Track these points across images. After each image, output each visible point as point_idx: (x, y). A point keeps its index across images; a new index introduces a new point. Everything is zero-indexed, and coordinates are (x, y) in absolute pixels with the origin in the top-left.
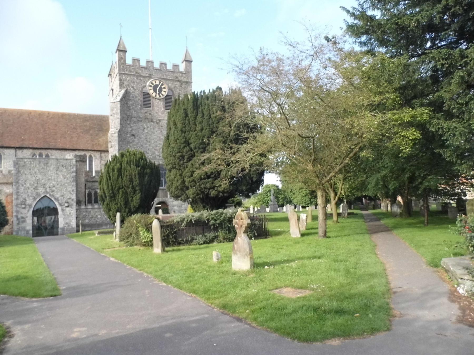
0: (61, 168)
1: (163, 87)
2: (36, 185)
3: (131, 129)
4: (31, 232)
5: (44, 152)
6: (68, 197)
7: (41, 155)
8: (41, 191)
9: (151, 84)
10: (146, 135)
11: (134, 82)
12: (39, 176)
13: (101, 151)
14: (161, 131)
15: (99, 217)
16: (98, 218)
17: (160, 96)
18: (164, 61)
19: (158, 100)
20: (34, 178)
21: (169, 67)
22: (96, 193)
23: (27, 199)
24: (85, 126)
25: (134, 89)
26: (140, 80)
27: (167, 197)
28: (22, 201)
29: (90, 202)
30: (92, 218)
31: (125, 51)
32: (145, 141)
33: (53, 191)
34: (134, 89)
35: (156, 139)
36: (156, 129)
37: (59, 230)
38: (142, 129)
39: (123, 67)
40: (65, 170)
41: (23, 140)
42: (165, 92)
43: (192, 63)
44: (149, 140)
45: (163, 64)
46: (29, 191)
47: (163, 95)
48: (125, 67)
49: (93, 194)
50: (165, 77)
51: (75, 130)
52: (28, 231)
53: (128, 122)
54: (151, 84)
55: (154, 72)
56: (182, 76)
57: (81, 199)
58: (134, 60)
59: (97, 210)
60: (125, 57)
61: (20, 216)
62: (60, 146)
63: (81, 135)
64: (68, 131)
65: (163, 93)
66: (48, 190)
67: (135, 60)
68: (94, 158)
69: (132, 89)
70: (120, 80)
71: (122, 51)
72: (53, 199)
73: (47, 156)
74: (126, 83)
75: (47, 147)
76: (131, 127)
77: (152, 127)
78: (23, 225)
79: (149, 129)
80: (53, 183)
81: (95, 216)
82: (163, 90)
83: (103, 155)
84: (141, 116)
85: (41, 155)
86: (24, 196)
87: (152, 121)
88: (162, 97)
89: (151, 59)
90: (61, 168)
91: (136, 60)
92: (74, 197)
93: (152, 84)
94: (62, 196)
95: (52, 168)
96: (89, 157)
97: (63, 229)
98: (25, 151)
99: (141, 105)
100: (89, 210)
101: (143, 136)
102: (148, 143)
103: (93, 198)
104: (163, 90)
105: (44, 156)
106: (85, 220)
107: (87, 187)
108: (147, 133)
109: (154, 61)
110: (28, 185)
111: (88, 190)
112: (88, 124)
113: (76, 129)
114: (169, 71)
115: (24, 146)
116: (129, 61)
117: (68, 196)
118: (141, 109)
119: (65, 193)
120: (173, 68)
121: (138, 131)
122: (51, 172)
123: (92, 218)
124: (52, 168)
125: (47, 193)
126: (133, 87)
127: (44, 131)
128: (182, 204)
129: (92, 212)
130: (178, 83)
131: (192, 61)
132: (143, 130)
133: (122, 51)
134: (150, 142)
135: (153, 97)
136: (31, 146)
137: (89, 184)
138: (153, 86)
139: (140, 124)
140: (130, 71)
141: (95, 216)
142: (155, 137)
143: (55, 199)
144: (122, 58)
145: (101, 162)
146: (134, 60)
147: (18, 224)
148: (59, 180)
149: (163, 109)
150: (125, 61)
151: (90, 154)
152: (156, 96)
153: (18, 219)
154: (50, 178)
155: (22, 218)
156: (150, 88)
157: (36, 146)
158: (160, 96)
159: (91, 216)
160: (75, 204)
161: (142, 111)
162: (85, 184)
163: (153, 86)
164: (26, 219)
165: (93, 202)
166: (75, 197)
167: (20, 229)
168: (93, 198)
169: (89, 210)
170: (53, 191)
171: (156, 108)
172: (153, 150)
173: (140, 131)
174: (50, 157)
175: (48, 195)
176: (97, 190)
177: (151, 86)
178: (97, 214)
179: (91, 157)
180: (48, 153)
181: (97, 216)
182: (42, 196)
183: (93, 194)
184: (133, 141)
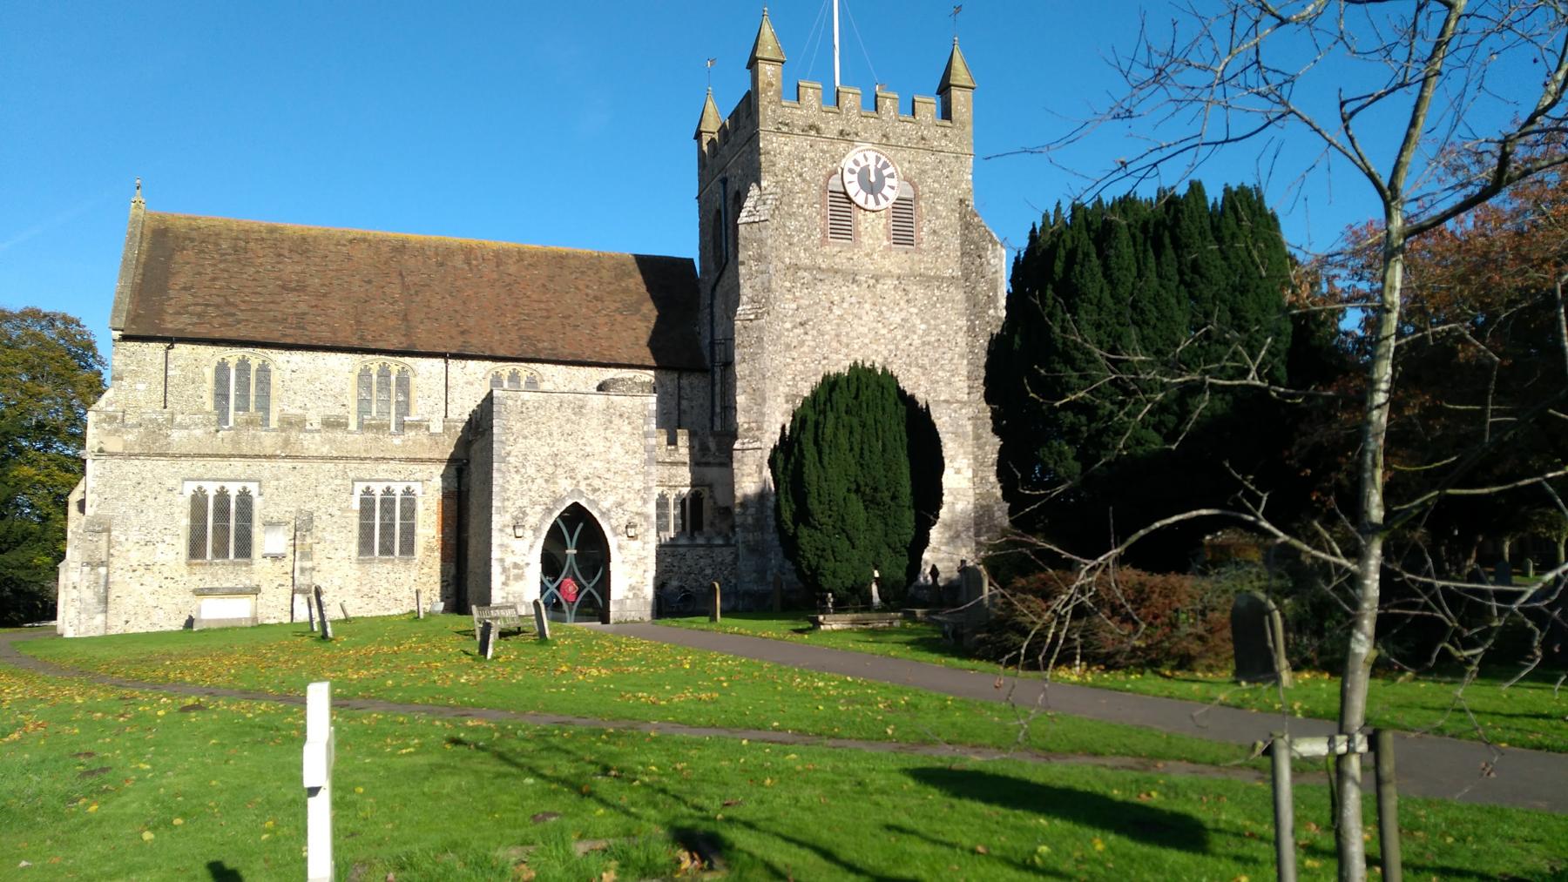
0: (616, 420)
2: (550, 470)
3: (794, 306)
5: (524, 369)
8: (564, 485)
12: (561, 446)
17: (878, 203)
20: (546, 448)
23: (528, 510)
24: (626, 291)
25: (804, 180)
26: (822, 151)
28: (515, 518)
32: (834, 344)
33: (595, 490)
34: (804, 180)
36: (867, 306)
40: (628, 429)
41: (463, 333)
44: (844, 340)
46: (535, 487)
51: (600, 305)
53: (788, 284)
59: (701, 551)
61: (508, 563)
62: (566, 352)
63: (620, 318)
65: (886, 191)
66: (583, 487)
69: (798, 180)
72: (596, 514)
73: (532, 385)
76: (795, 299)
77: (854, 300)
78: (515, 587)
79: (845, 305)
80: (595, 464)
83: (684, 382)
84: (823, 266)
85: (514, 377)
86: (518, 504)
87: (854, 281)
88: (883, 204)
90: (616, 420)
94: (619, 505)
95: (594, 423)
97: (621, 602)
98: (472, 365)
99: (823, 231)
100: (682, 550)
101: (828, 327)
102: (844, 350)
104: (888, 181)
108: (841, 317)
110: (531, 471)
117: (634, 505)
118: (823, 242)
119: (627, 496)
122: (592, 434)
124: (594, 423)
125: (581, 493)
127: (516, 305)
130: (929, 158)
132: (830, 310)
134: (848, 345)
139: (822, 288)
142: (861, 329)
145: (679, 404)
148: (612, 456)
149: (886, 243)
153: (504, 570)
154: (588, 449)
155: (516, 566)
158: (878, 203)
159: (685, 569)
161: (827, 249)
163: (857, 169)
169: (682, 550)
170: (595, 490)
171: (865, 240)
173: (821, 312)
175: (583, 503)
177: (852, 171)
178: (702, 562)
181: (702, 570)
182: (569, 503)
184: (802, 343)
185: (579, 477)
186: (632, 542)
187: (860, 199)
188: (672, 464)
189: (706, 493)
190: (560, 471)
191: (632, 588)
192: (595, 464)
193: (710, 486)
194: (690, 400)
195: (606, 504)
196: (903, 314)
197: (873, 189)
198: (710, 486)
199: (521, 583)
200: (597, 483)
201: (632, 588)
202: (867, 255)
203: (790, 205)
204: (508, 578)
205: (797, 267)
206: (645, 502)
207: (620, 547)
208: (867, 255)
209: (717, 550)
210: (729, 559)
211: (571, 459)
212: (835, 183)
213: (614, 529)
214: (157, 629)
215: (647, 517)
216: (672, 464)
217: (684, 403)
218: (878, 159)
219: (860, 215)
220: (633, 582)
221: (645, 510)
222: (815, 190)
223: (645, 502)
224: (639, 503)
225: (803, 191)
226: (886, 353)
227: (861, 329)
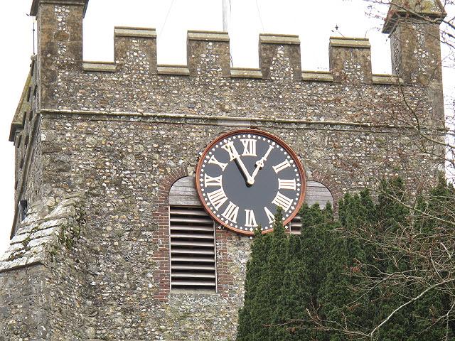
1: (277, 169)
9: (213, 160)
18: (280, 27)
21: (315, 59)
26: (155, 138)
39: (69, 81)
42: (288, 193)
54: (213, 160)
55: (229, 94)
58: (123, 38)
60: (77, 28)
65: (280, 200)
67: (129, 37)
69: (111, 191)
82: (283, 184)
93: (223, 156)
99: (159, 277)
109: (232, 38)
114: (314, 81)
116: (98, 47)
118: (158, 299)
120: (333, 62)
126: (117, 183)
138: (223, 166)
140: (104, 102)
146: (123, 38)
150: (77, 50)
156: (208, 180)
177: (214, 171)
187: (230, 215)
212: (181, 192)
218: (261, 150)
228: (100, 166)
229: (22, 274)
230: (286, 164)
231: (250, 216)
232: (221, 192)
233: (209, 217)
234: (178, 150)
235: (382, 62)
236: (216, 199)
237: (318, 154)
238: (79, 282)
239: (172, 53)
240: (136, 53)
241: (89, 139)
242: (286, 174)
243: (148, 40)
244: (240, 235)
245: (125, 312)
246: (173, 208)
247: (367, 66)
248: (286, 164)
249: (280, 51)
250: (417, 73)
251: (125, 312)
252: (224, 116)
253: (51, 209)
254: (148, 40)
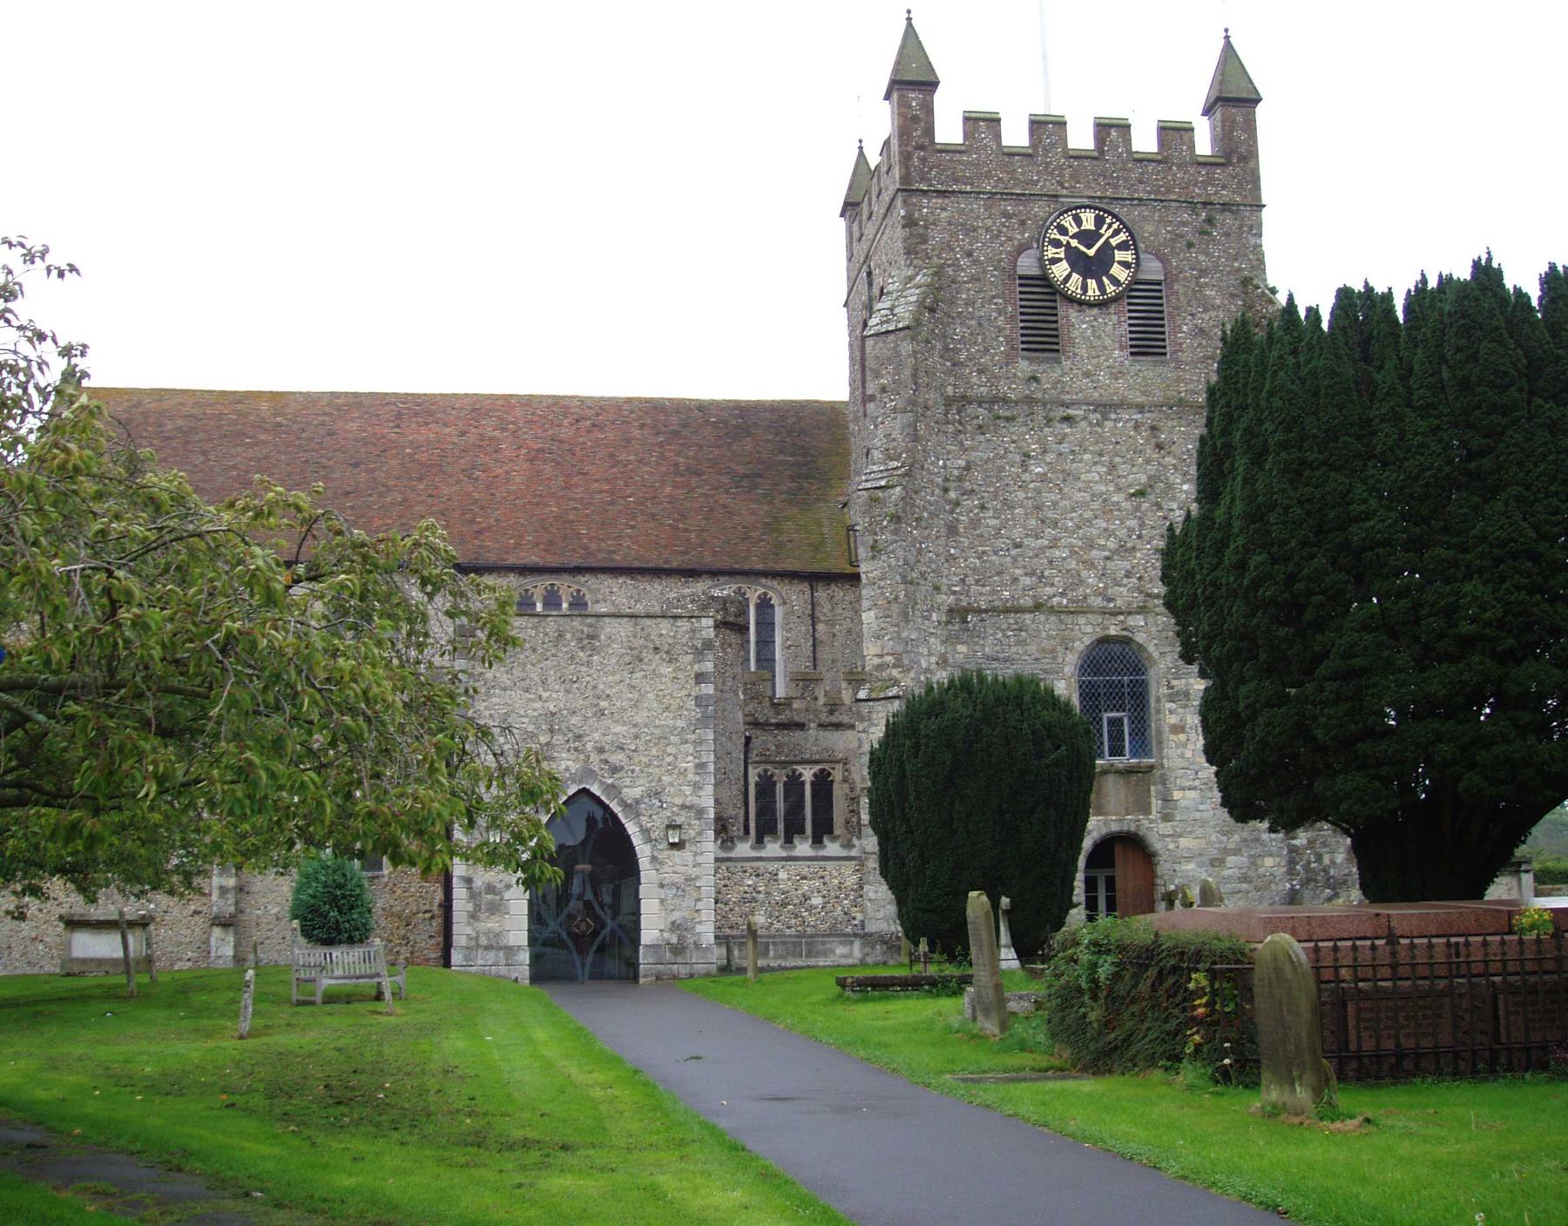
0: (647, 655)
2: (543, 739)
4: (525, 957)
5: (566, 587)
6: (678, 801)
7: (552, 600)
10: (1038, 491)
11: (975, 230)
13: (815, 579)
14: (1113, 467)
15: (817, 901)
16: (810, 909)
19: (1095, 311)
20: (538, 705)
21: (1145, 141)
22: (794, 783)
27: (1146, 810)
29: (765, 830)
30: (784, 905)
31: (934, 84)
32: (1033, 522)
33: (615, 770)
34: (976, 262)
35: (1086, 505)
36: (1087, 457)
37: (644, 958)
38: (1018, 459)
39: (923, 160)
40: (666, 670)
43: (1260, 110)
45: (1111, 131)
47: (1115, 281)
48: (932, 160)
49: (780, 788)
50: (1125, 193)
51: (694, 481)
52: (510, 950)
56: (1209, 181)
57: (731, 812)
60: (929, 109)
61: (478, 883)
64: (663, 483)
65: (1116, 270)
67: (977, 120)
68: (779, 613)
70: (910, 222)
71: (913, 83)
72: (616, 807)
73: (578, 603)
74: (936, 237)
75: (577, 561)
77: (1064, 448)
79: (1050, 457)
81: (796, 897)
82: (1119, 255)
83: (822, 594)
89: (1055, 110)
90: (647, 655)
91: (982, 124)
92: (707, 800)
96: (758, 606)
100: (772, 866)
101: (1021, 495)
103: (781, 806)
104: (1119, 255)
105: (565, 605)
106: (752, 912)
107: (753, 756)
108: (1043, 478)
111: (760, 769)
112: (748, 445)
113: (698, 474)
114: (1142, 160)
115: (491, 558)
116: (948, 131)
118: (1009, 359)
121: (1001, 469)
123: (784, 905)
125: (590, 773)
126: (969, 254)
128: (1226, 851)
129: (782, 875)
131: (1258, 100)
132: (1024, 467)
133: (913, 83)
134: (1055, 524)
135: (1071, 300)
136: (511, 560)
137: (763, 740)
140: (956, 181)
141: (796, 897)
142: (1079, 496)
143: (625, 806)
144: (915, 119)
147: (473, 916)
148: (641, 717)
150: (929, 131)
151: (761, 591)
152: (1085, 288)
153: (473, 896)
154: (604, 704)
155: (490, 888)
156: (1051, 252)
157: (534, 559)
160: (711, 834)
162: (748, 740)
164: (507, 895)
165: (781, 826)
166: (711, 802)
167: (483, 941)
168: (781, 806)
172: (1073, 564)
174: (594, 608)
175: (595, 789)
176: (800, 768)
178: (805, 886)
179: (765, 605)
180: (584, 590)
181: (806, 898)
183: (780, 788)
185: (590, 746)
186: (676, 853)
188: (781, 726)
189: (837, 774)
190: (558, 739)
191: (675, 927)
192: (618, 729)
193: (845, 762)
194: (828, 622)
195: (632, 793)
196: (1151, 469)
197: (1093, 267)
198: (845, 762)
199: (496, 918)
200: (617, 758)
201: (675, 927)
202: (1087, 374)
203: (952, 302)
204: (477, 907)
205: (965, 400)
206: (697, 787)
207: (654, 859)
208: (1087, 374)
209: (830, 865)
210: (851, 880)
211: (574, 720)
212: (1027, 264)
213: (645, 832)
214: (36, 970)
215: (700, 813)
216: (781, 726)
217: (820, 627)
219: (1073, 314)
220: (676, 916)
221: (696, 800)
222: (992, 275)
223: (697, 787)
224: (688, 790)
225: (974, 279)
226: (1122, 533)
227: (1079, 496)
228: (954, 235)
229: (891, 337)
230: (1123, 237)
231: (1092, 283)
232: (1064, 265)
233: (1050, 286)
234: (1023, 223)
235: (1204, 145)
236: (1060, 270)
237: (1150, 228)
238: (939, 346)
239: (1015, 135)
240: (984, 136)
241: (944, 214)
242: (1123, 246)
243: (993, 122)
244: (1081, 303)
245: (980, 372)
246: (1021, 278)
247: (1192, 147)
248: (1123, 237)
249: (1114, 133)
250: (1238, 151)
251: (980, 372)
252: (1065, 192)
253: (911, 278)
254: (993, 122)
